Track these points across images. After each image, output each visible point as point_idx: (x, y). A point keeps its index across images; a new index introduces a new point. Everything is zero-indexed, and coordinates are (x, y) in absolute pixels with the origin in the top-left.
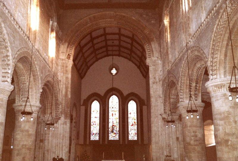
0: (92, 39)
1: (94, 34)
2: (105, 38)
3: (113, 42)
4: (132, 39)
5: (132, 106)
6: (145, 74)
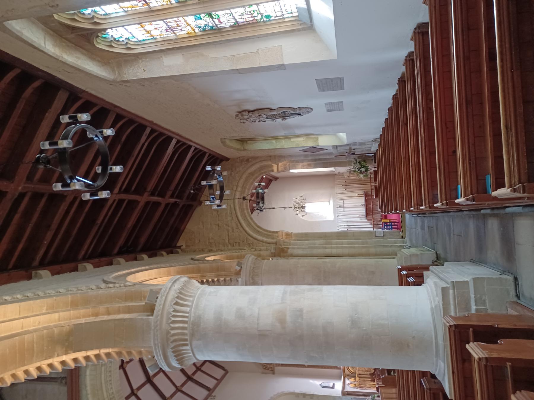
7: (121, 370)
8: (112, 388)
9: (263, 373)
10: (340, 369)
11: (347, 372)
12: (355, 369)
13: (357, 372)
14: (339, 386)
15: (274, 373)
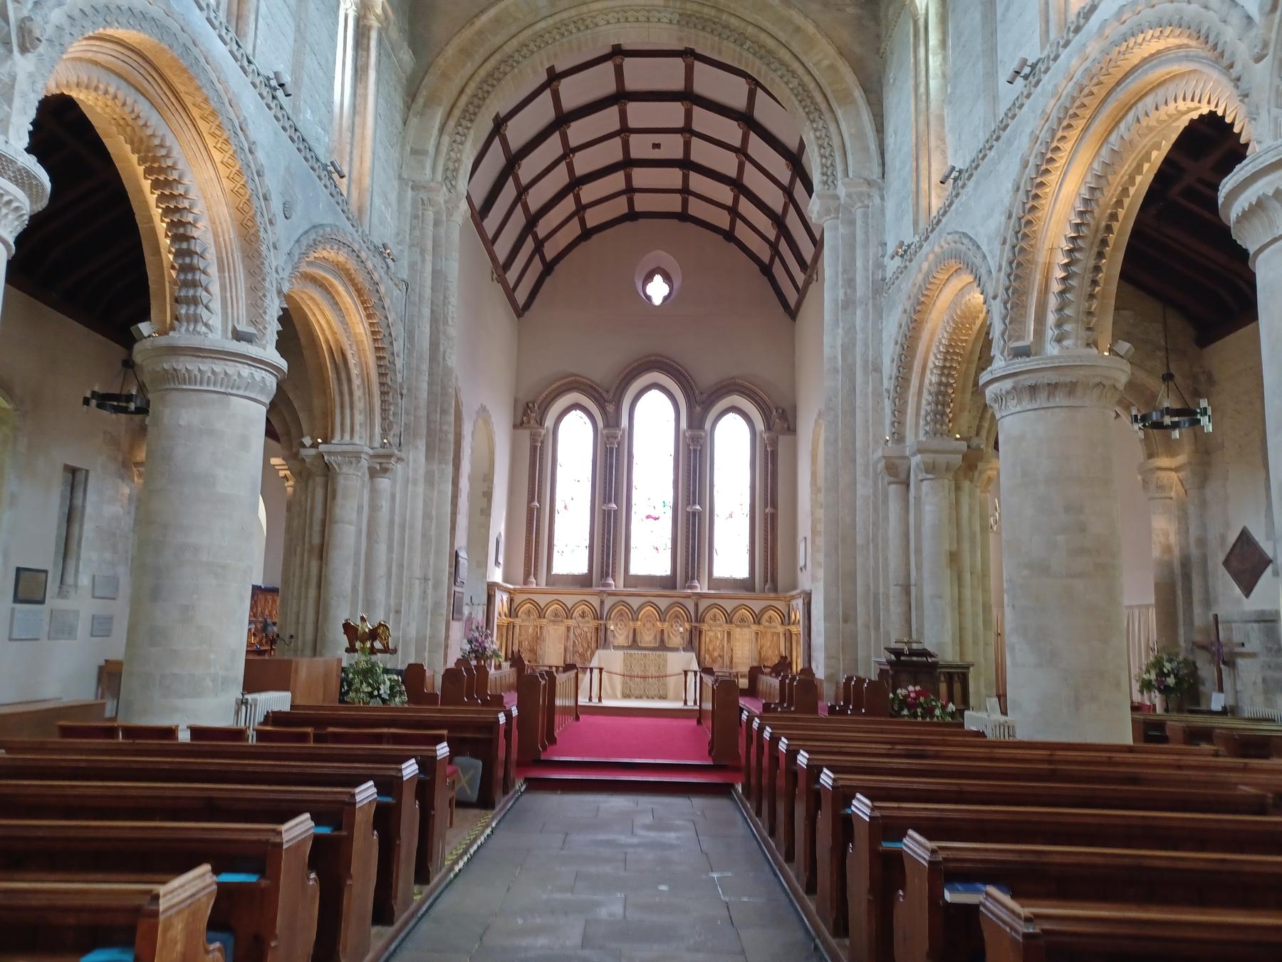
0: (562, 120)
1: (574, 92)
2: (628, 179)
3: (657, 146)
4: (747, 120)
5: (733, 439)
6: (792, 297)
7: (608, 50)
8: (608, 23)
9: (516, 401)
10: (526, 582)
11: (519, 598)
12: (524, 616)
13: (518, 621)
14: (496, 575)
15: (515, 427)
